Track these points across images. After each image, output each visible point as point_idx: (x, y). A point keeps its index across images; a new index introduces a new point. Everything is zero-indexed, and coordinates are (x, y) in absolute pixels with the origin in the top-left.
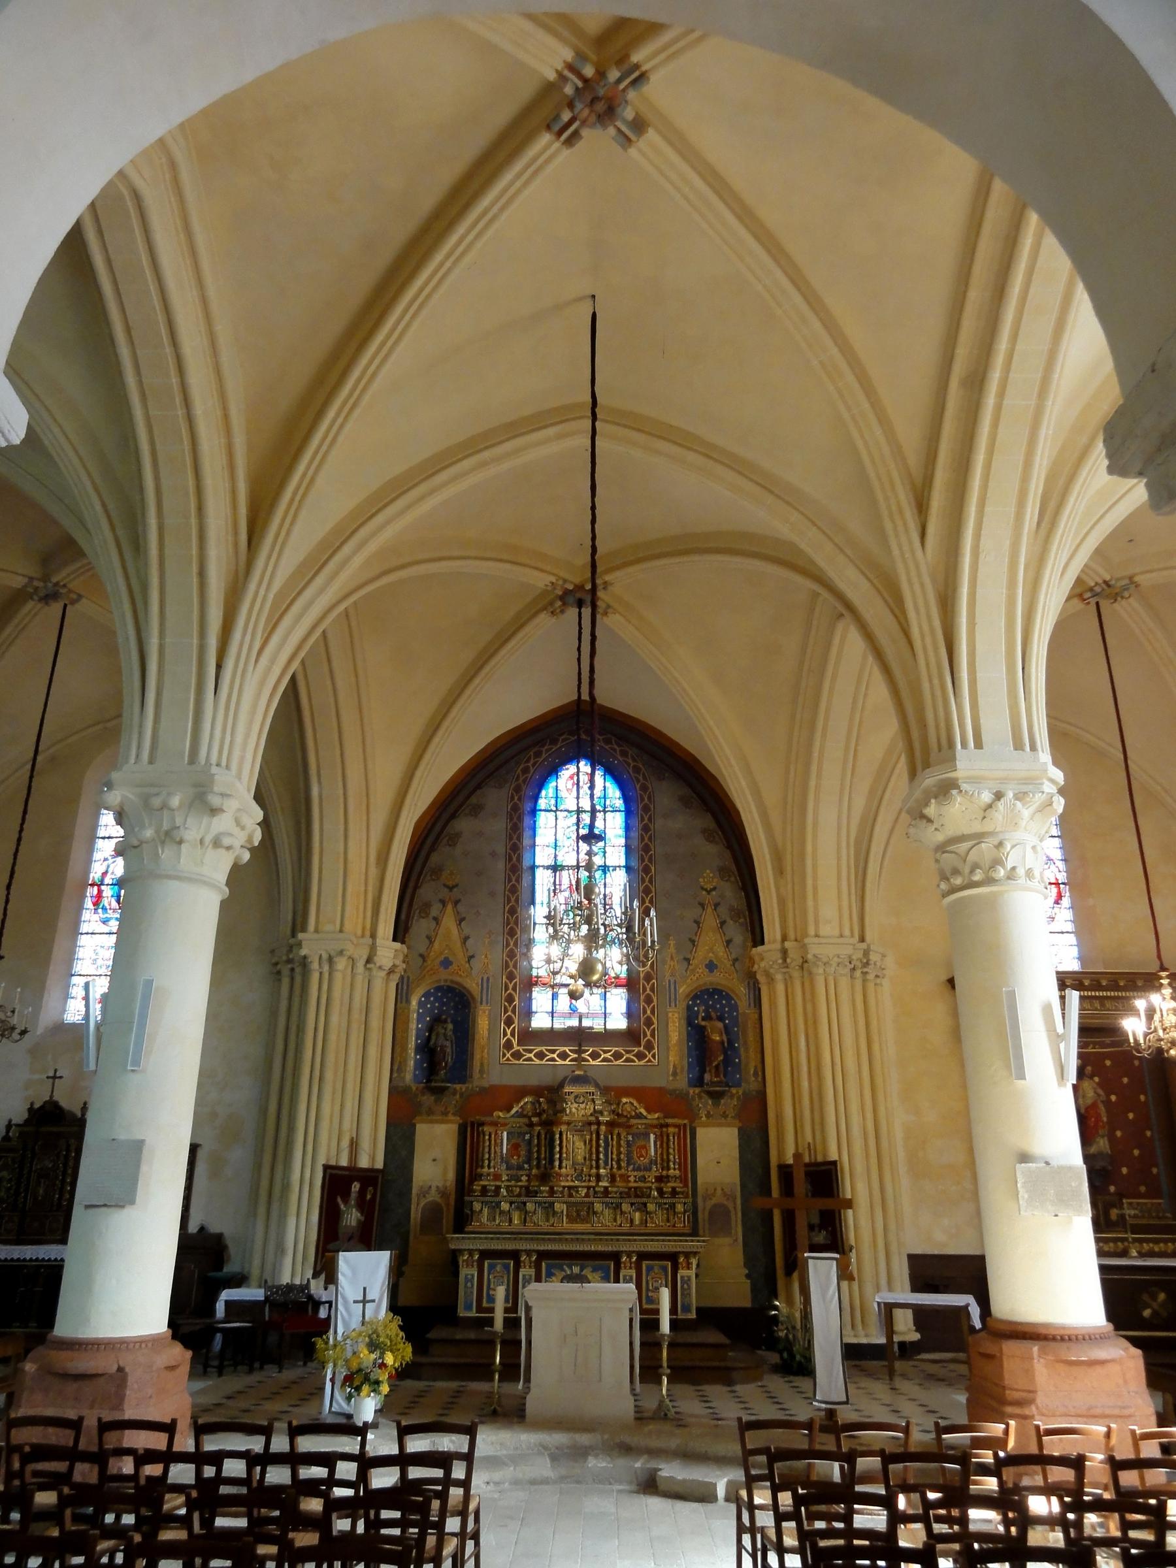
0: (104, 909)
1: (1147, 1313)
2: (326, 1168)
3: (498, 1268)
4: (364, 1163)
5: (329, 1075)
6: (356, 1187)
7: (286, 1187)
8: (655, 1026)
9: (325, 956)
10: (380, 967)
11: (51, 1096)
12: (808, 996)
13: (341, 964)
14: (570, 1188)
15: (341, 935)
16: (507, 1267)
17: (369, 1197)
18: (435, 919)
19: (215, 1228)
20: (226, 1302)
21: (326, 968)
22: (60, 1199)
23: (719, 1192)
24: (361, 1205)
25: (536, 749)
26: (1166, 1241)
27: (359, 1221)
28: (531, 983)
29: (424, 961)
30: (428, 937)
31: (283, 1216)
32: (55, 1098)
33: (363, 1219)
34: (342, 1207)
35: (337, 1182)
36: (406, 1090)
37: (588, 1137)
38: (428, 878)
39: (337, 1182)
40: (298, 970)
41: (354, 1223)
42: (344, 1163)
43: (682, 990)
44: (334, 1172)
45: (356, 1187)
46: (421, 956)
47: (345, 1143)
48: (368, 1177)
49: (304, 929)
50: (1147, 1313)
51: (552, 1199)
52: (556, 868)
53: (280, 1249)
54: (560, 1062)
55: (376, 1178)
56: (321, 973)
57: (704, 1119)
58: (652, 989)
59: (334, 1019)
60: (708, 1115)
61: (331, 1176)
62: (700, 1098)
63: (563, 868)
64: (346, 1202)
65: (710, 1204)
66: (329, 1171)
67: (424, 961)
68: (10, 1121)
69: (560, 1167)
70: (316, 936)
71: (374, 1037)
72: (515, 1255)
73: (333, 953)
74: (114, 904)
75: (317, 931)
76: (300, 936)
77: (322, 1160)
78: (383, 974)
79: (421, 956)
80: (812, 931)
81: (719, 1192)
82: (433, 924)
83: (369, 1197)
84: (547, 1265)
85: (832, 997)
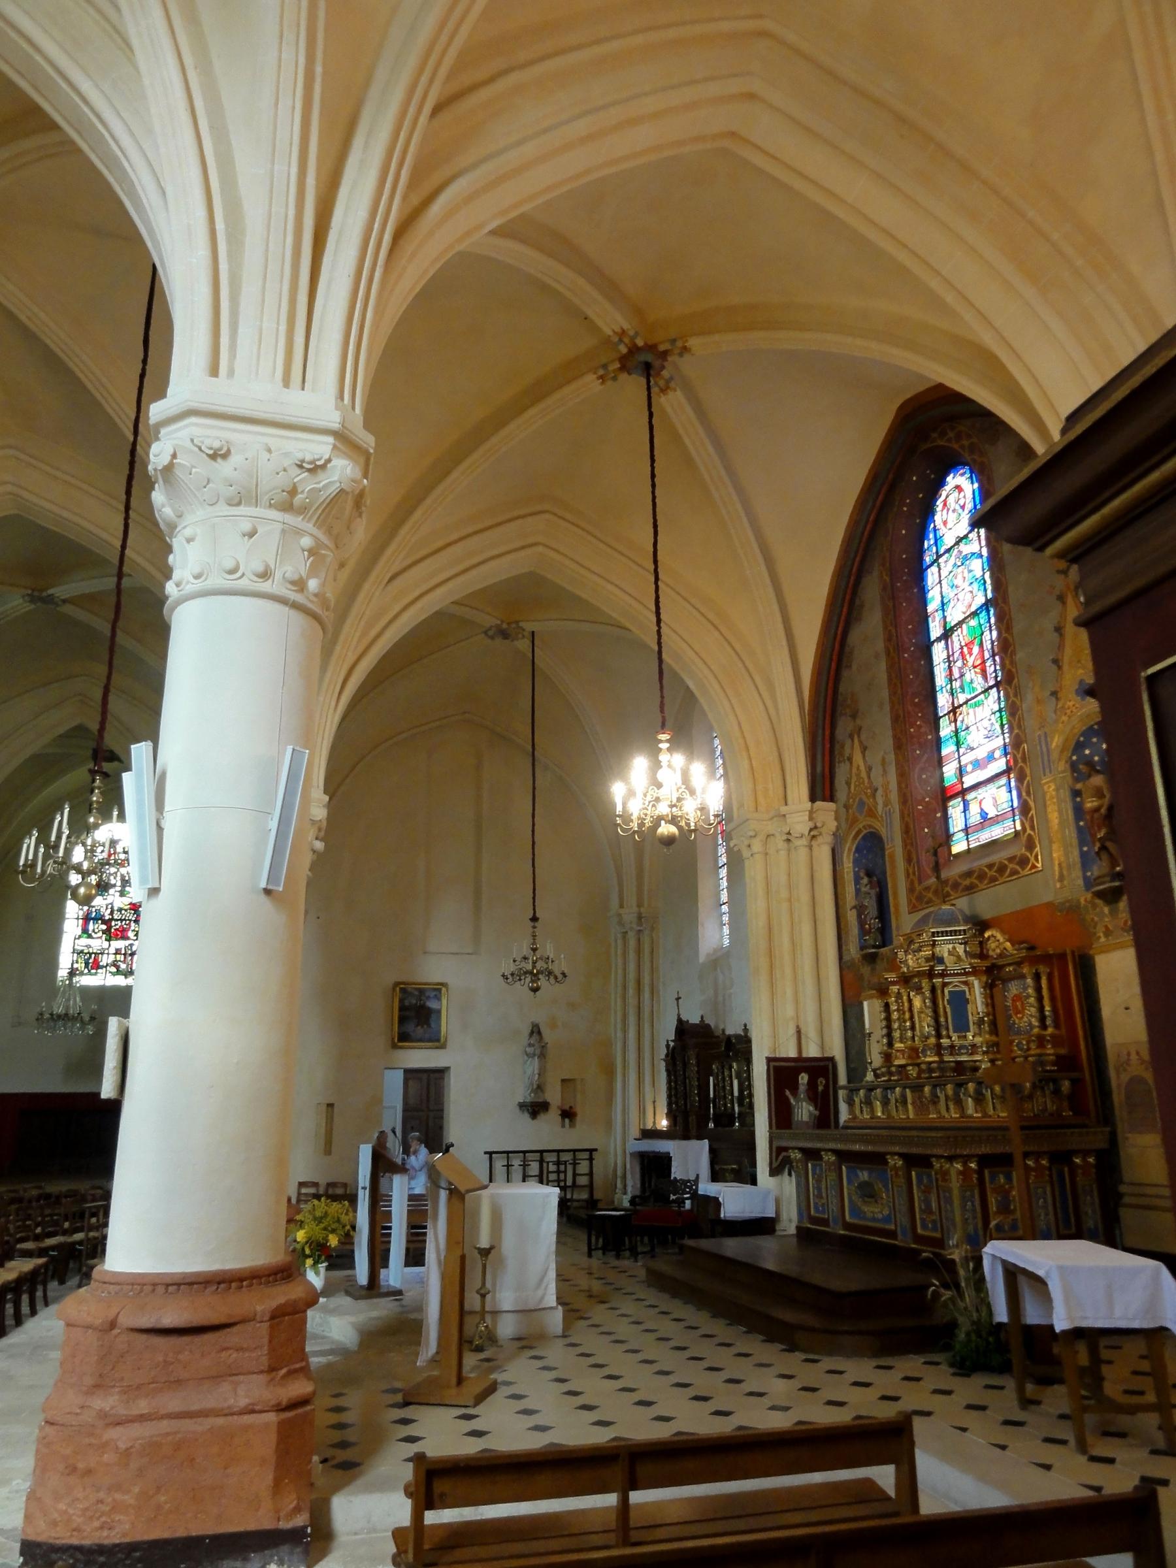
2: (769, 1060)
4: (812, 1051)
6: (804, 1078)
8: (1033, 812)
17: (820, 1088)
23: (1134, 1057)
24: (813, 1095)
27: (811, 1114)
28: (945, 796)
33: (817, 1113)
34: (792, 1101)
41: (805, 1118)
42: (792, 1053)
43: (1056, 741)
44: (777, 1064)
45: (804, 1078)
48: (821, 1068)
57: (1103, 939)
58: (1024, 759)
60: (1108, 932)
61: (775, 1067)
62: (1094, 906)
65: (1125, 1078)
66: (772, 1064)
78: (804, 842)
81: (1134, 1057)
83: (820, 1088)
84: (990, 1173)
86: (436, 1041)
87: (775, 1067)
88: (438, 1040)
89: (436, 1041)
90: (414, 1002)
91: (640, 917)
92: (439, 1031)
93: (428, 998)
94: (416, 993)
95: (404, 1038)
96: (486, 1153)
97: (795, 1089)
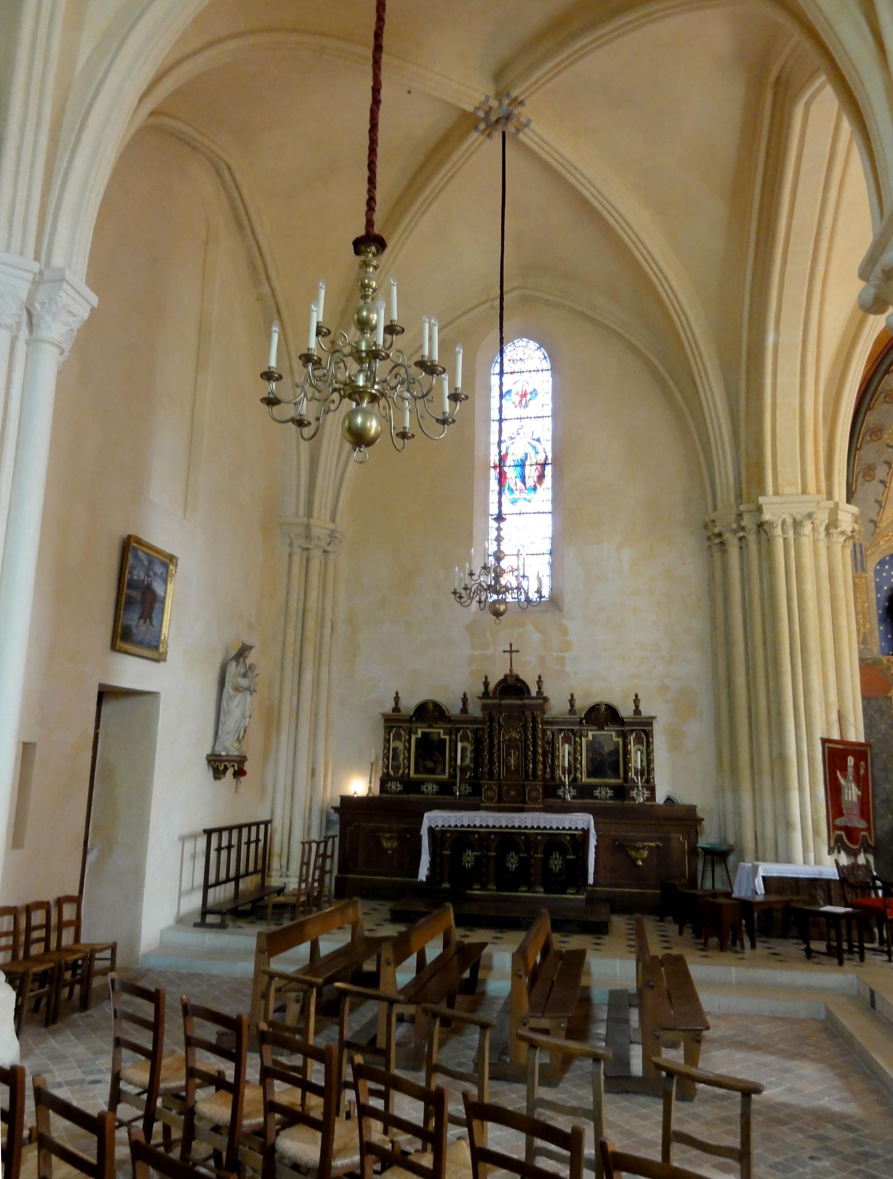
0: (511, 490)
2: (824, 741)
5: (813, 644)
6: (851, 761)
7: (781, 759)
9: (789, 521)
10: (843, 533)
11: (511, 671)
13: (807, 529)
15: (805, 497)
18: (883, 482)
19: (685, 798)
20: (764, 878)
21: (791, 534)
22: (535, 769)
29: (876, 526)
30: (878, 502)
31: (784, 790)
32: (515, 672)
33: (860, 793)
34: (842, 781)
35: (836, 756)
36: (876, 663)
38: (868, 438)
39: (836, 756)
40: (752, 539)
41: (855, 799)
42: (836, 736)
44: (831, 745)
45: (851, 761)
46: (872, 521)
47: (834, 717)
48: (860, 752)
49: (763, 493)
53: (789, 826)
55: (865, 752)
56: (785, 539)
59: (810, 588)
64: (845, 777)
66: (827, 745)
67: (876, 526)
68: (465, 694)
70: (777, 499)
71: (842, 605)
73: (799, 518)
74: (520, 485)
75: (776, 493)
76: (761, 500)
77: (819, 733)
79: (872, 521)
82: (882, 487)
86: (154, 650)
87: (829, 748)
88: (157, 648)
89: (154, 650)
90: (142, 576)
91: (332, 534)
92: (160, 631)
93: (155, 574)
94: (146, 563)
95: (123, 638)
96: (205, 831)
97: (844, 769)
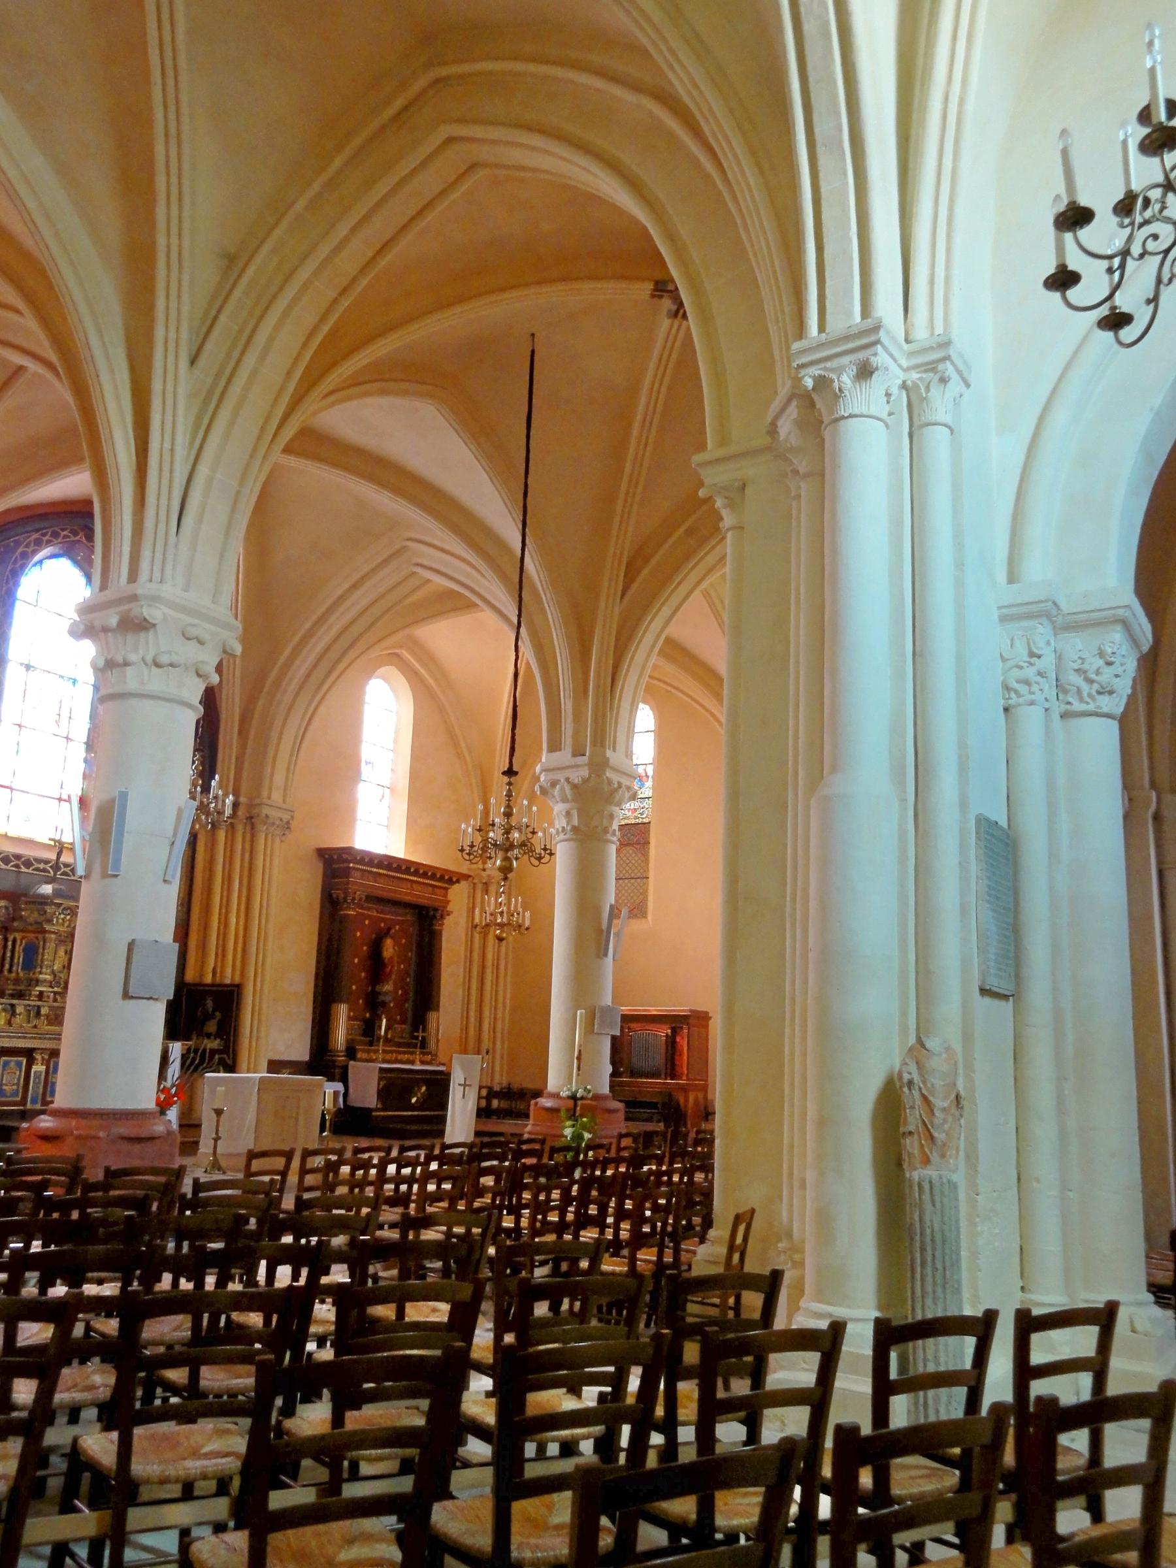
1: (414, 1100)
3: (12, 1065)
12: (247, 846)
14: (55, 993)
16: (19, 1064)
25: (36, 536)
26: (404, 1053)
37: (69, 948)
50: (414, 1100)
51: (40, 1003)
52: (28, 667)
54: (23, 869)
63: (36, 668)
69: (10, 971)
72: (29, 1053)
80: (265, 793)
85: (268, 852)
